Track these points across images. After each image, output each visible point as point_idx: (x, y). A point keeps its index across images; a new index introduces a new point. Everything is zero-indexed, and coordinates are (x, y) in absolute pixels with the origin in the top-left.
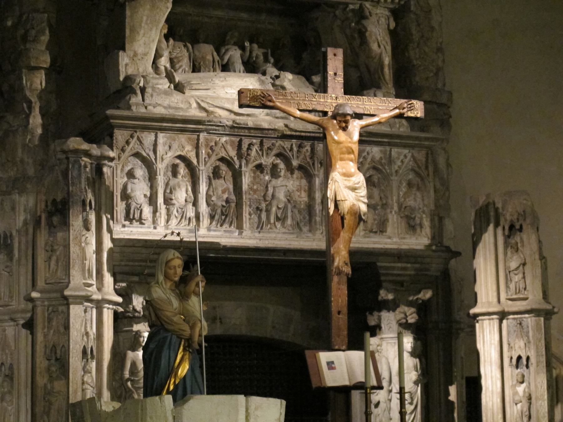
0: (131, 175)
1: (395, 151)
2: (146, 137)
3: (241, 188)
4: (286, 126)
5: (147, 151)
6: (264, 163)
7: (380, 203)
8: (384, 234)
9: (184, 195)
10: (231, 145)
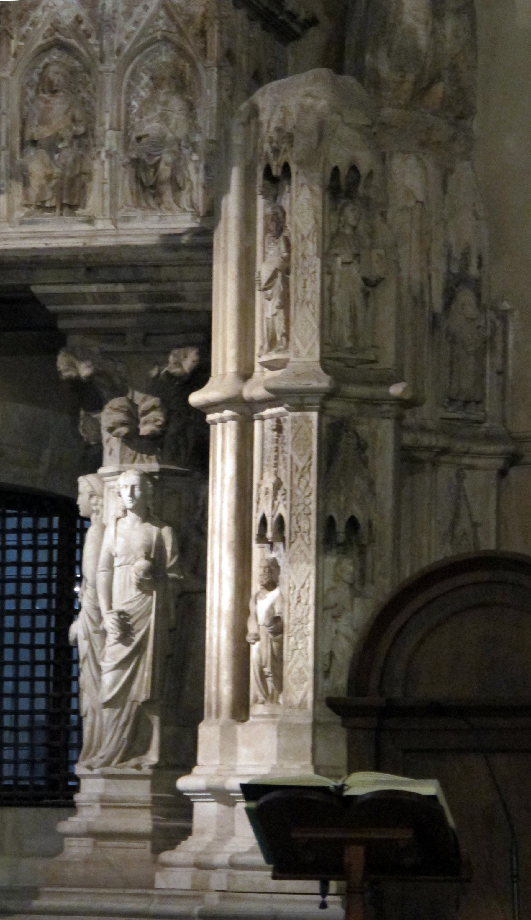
7: (68, 134)
8: (79, 211)
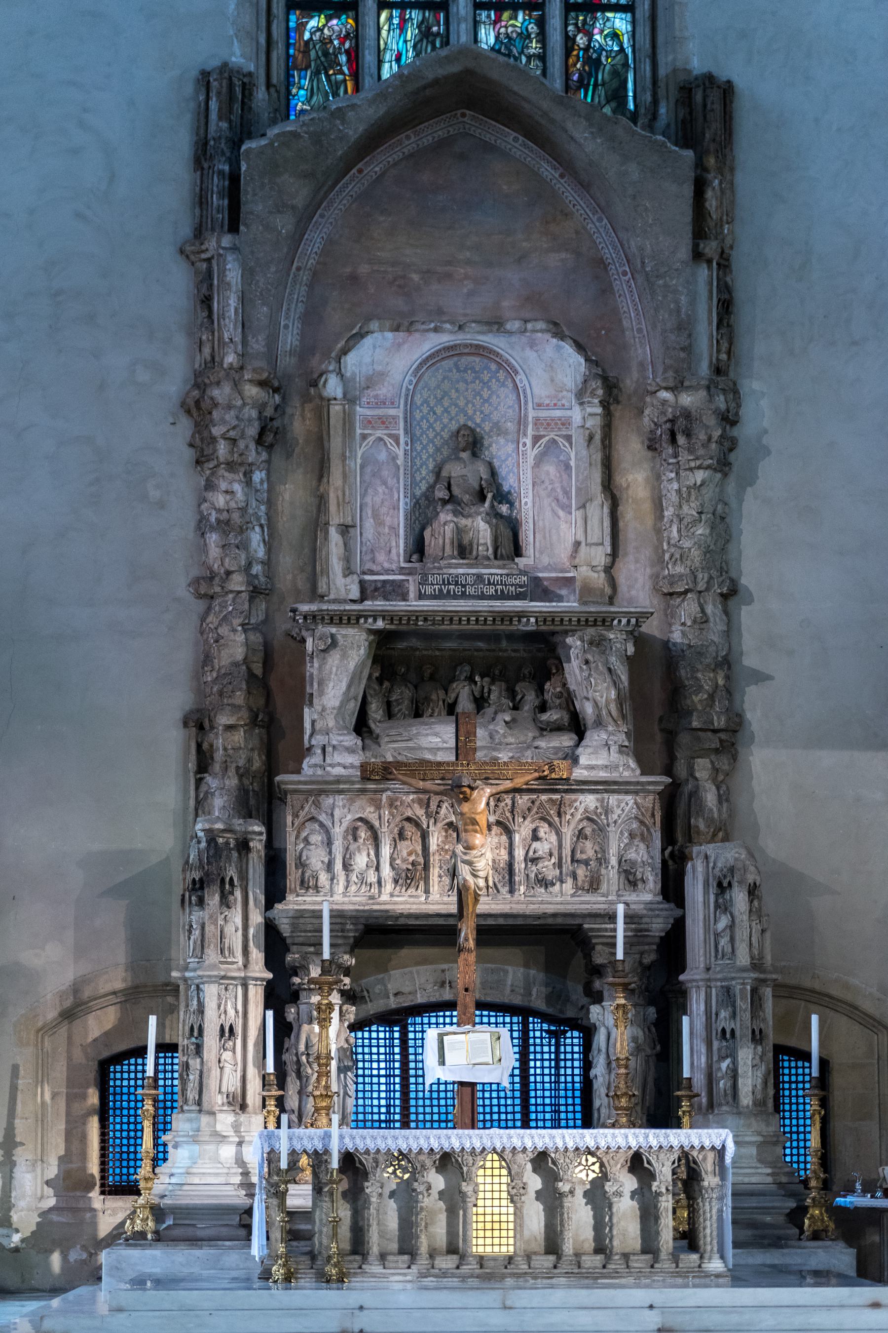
0: (306, 840)
1: (613, 800)
9: (366, 859)
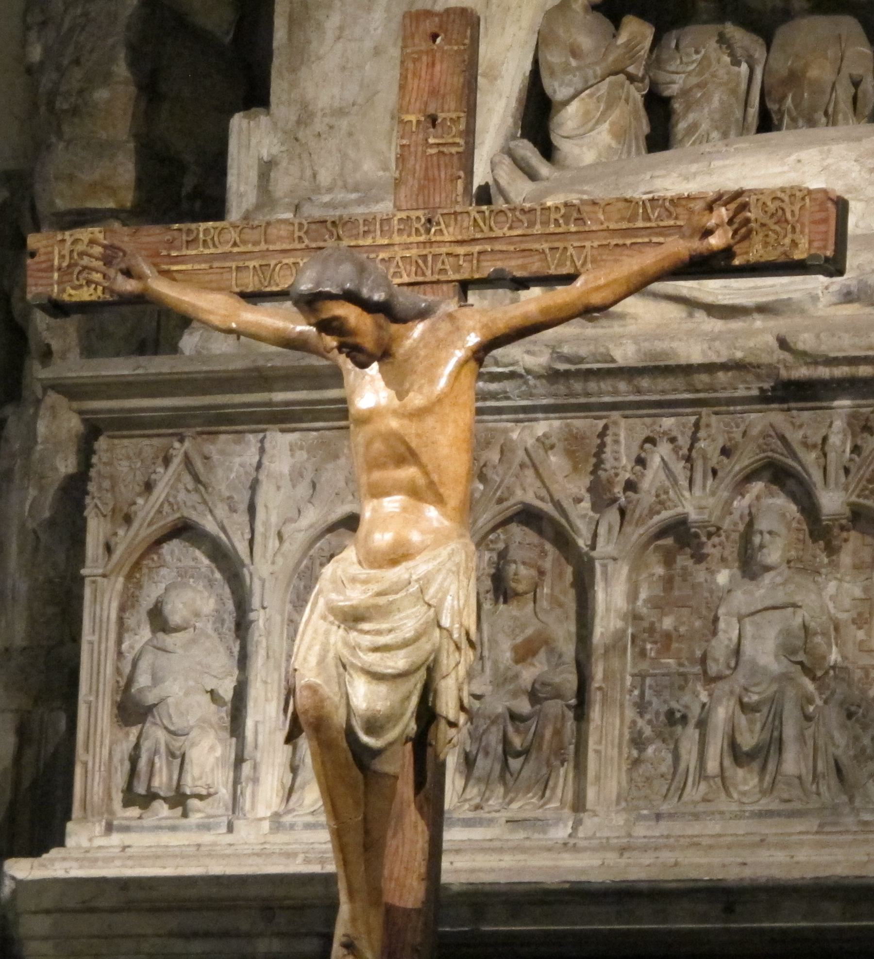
0: (158, 619)
2: (222, 452)
3: (591, 633)
4: (783, 343)
5: (221, 511)
6: (693, 516)
10: (570, 454)
